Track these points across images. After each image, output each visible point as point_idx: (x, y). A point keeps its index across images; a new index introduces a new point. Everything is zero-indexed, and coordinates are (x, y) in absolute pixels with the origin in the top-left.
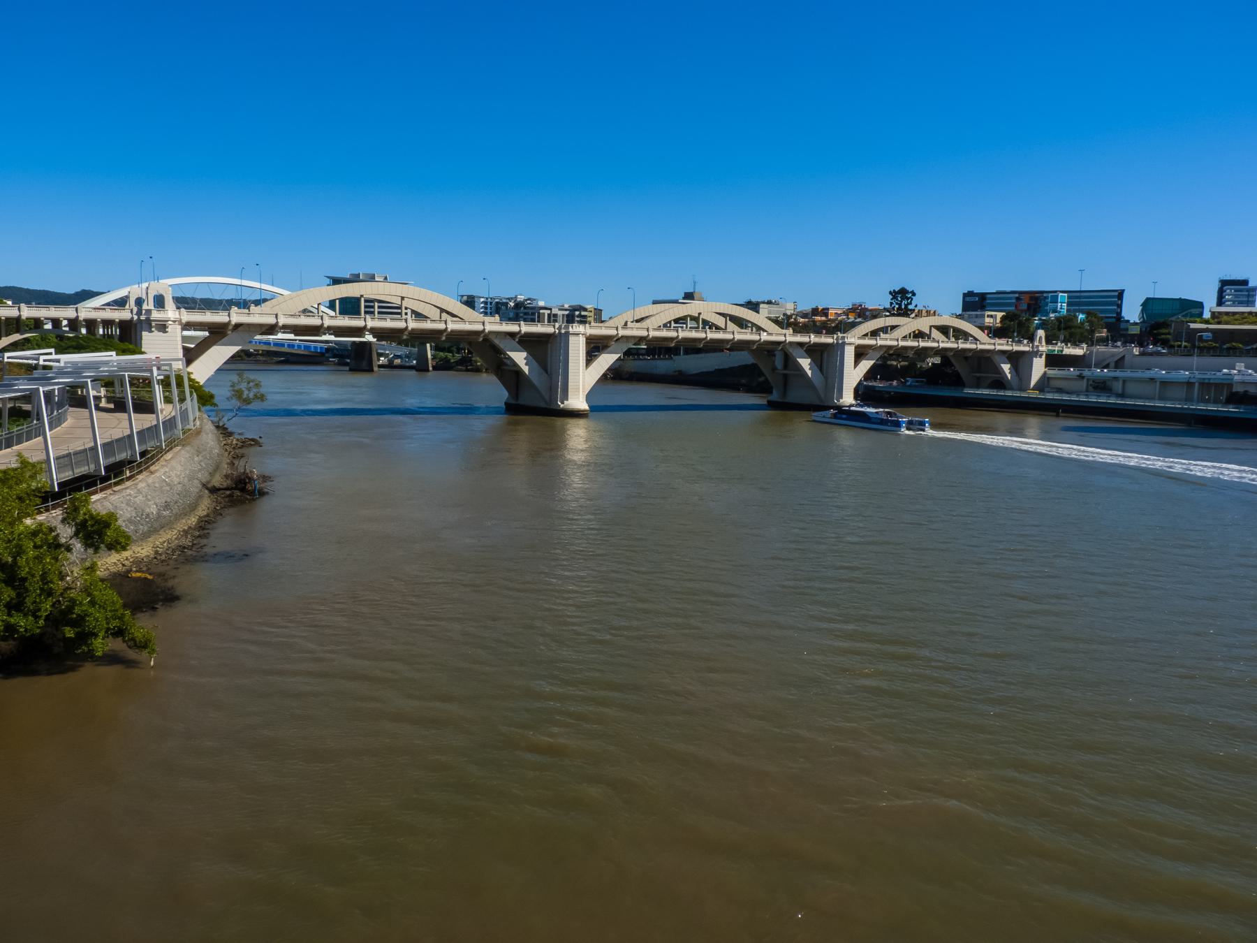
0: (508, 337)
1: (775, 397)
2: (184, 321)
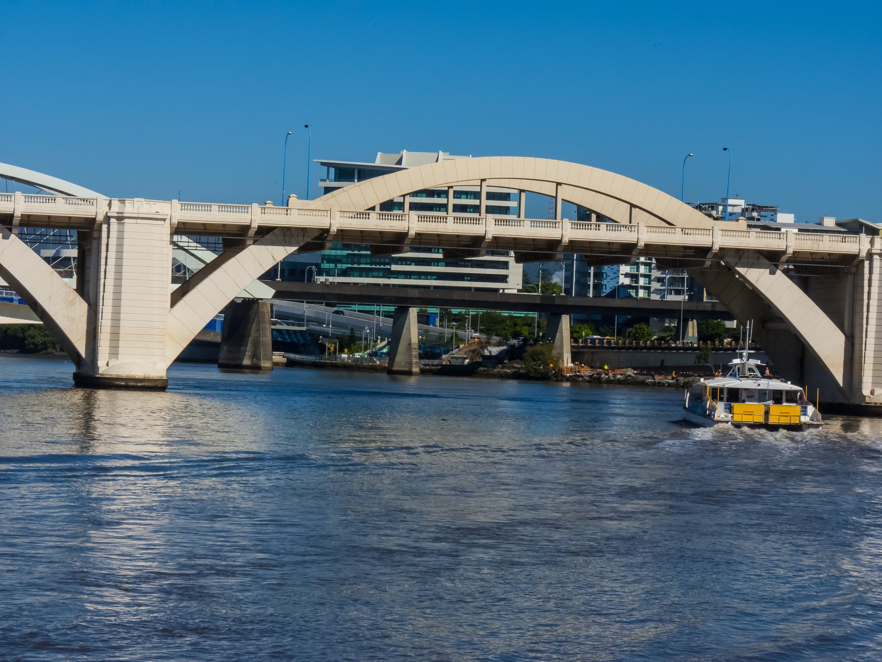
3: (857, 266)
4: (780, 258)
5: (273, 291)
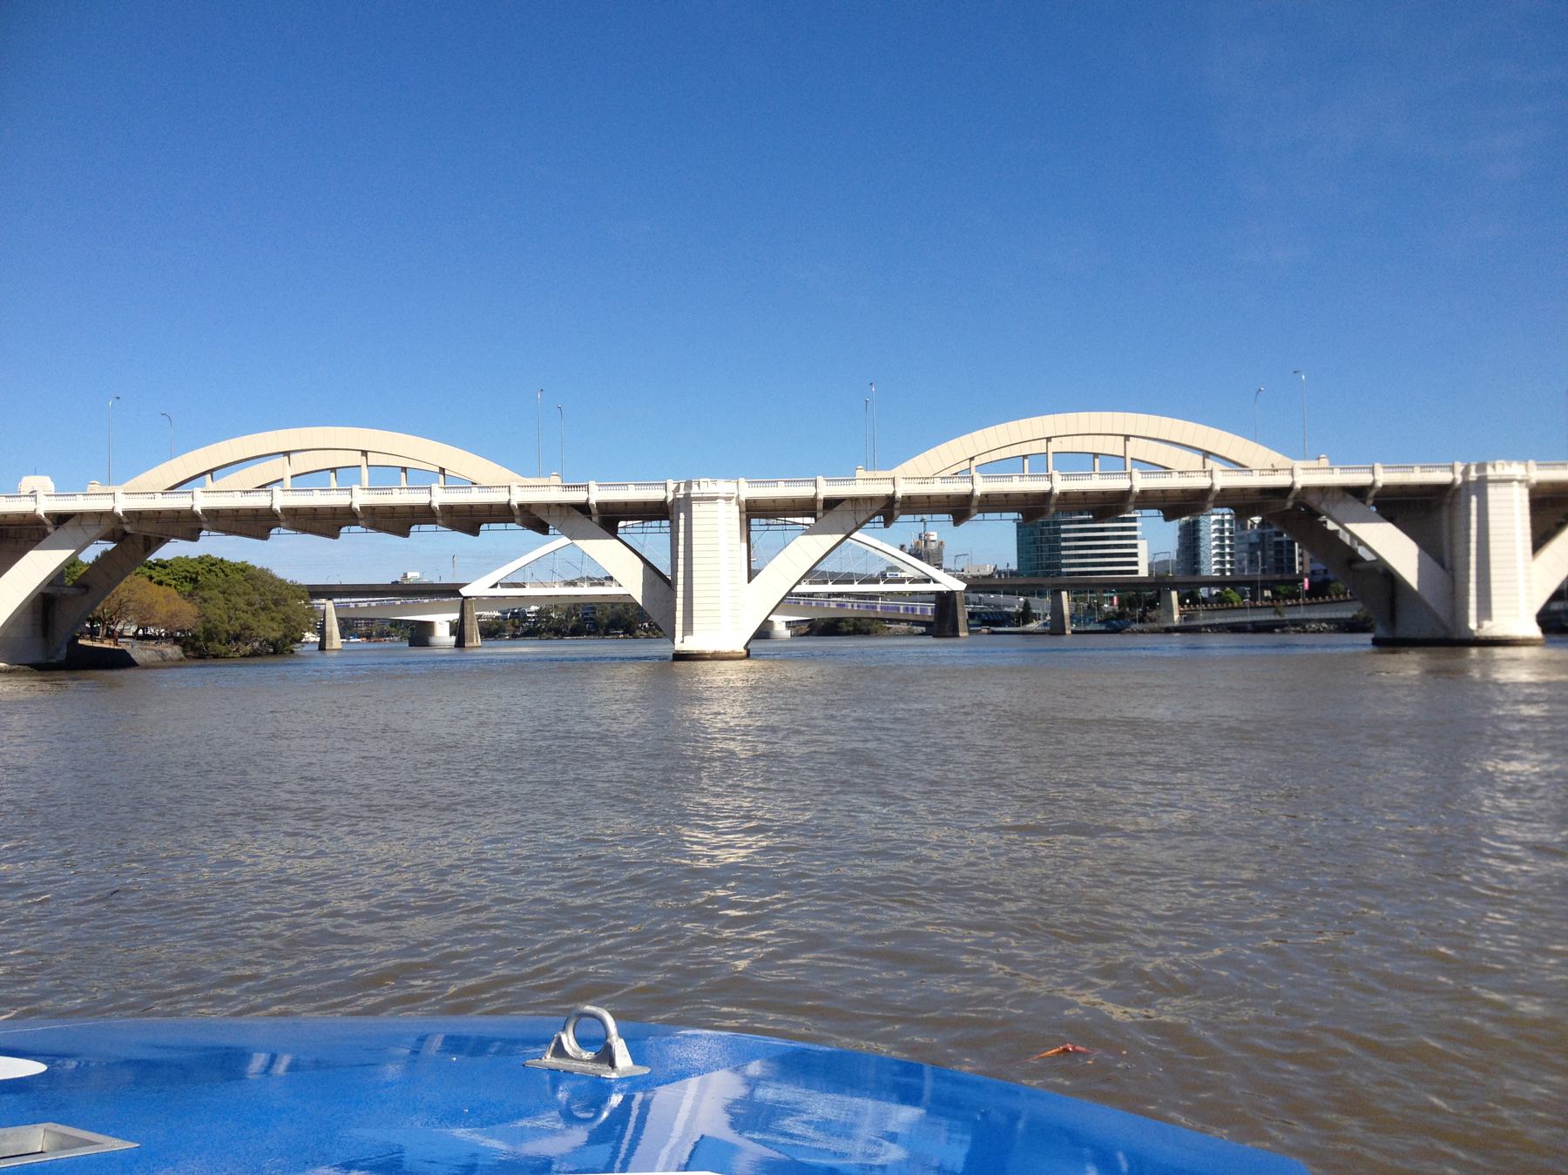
1: (1381, 632)
3: (1453, 496)
4: (1367, 493)
5: (964, 586)
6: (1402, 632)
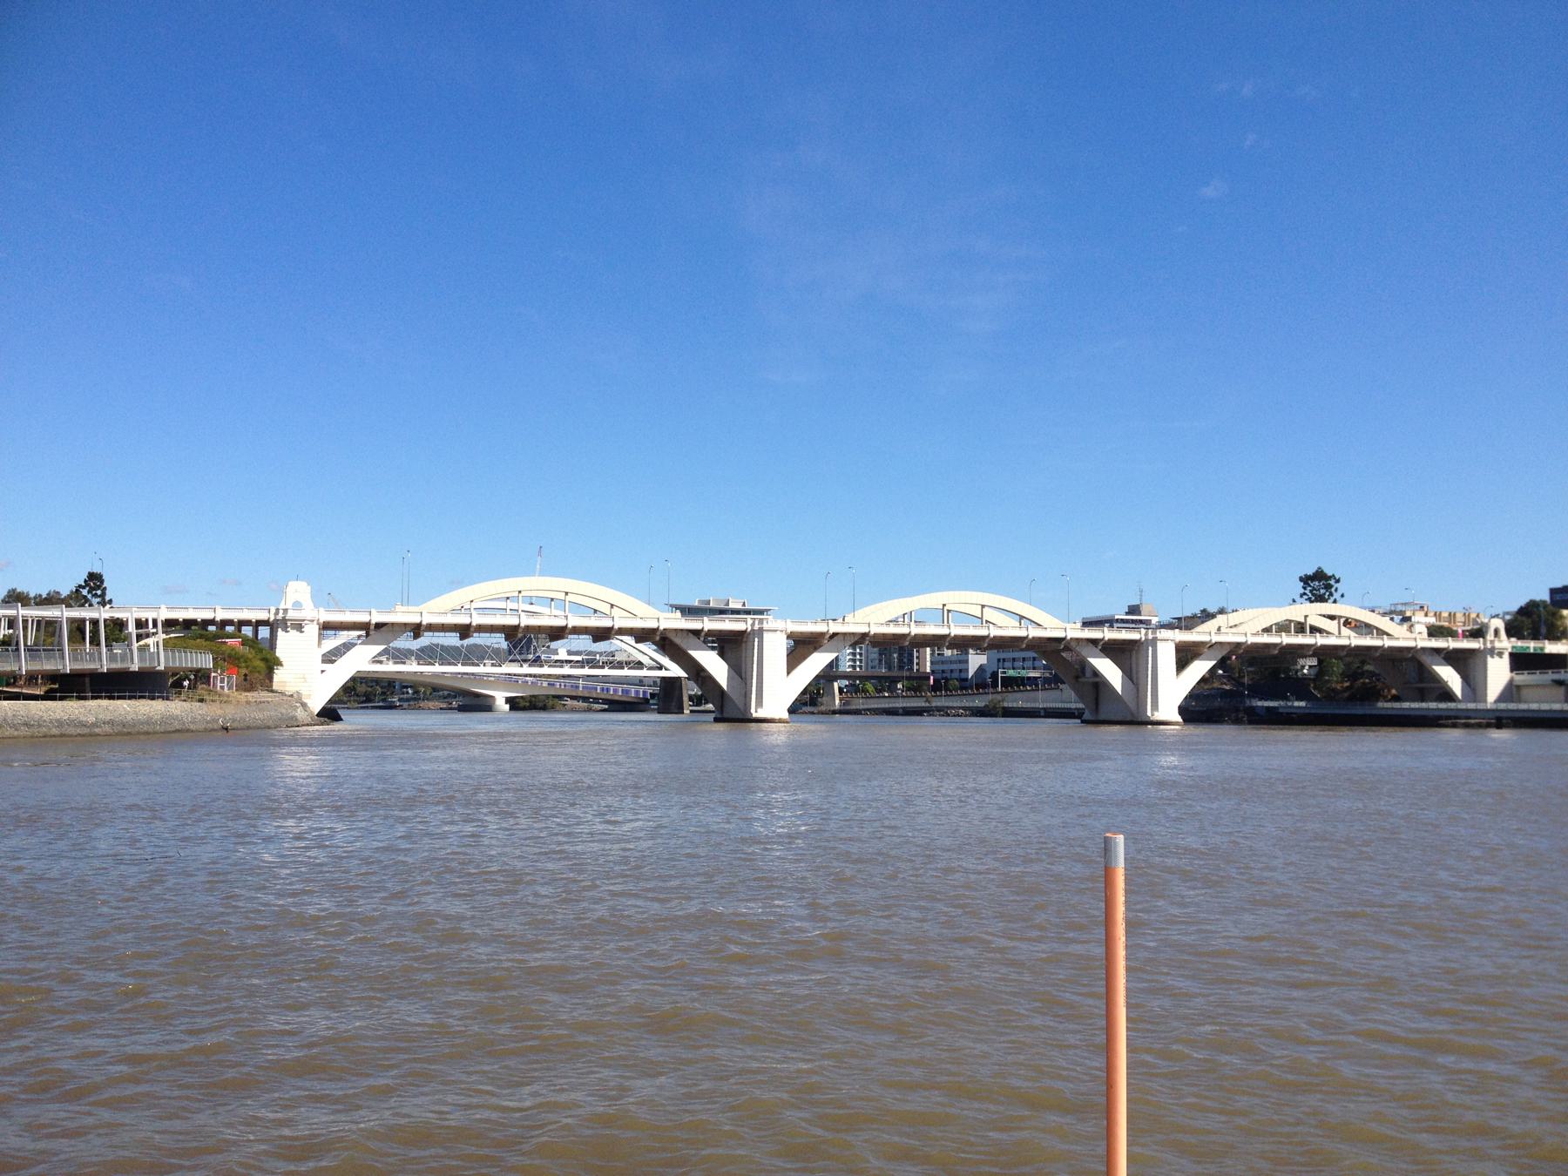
0: (691, 635)
2: (321, 621)
6: (1102, 717)
